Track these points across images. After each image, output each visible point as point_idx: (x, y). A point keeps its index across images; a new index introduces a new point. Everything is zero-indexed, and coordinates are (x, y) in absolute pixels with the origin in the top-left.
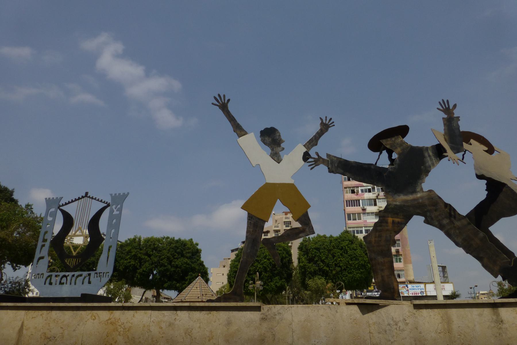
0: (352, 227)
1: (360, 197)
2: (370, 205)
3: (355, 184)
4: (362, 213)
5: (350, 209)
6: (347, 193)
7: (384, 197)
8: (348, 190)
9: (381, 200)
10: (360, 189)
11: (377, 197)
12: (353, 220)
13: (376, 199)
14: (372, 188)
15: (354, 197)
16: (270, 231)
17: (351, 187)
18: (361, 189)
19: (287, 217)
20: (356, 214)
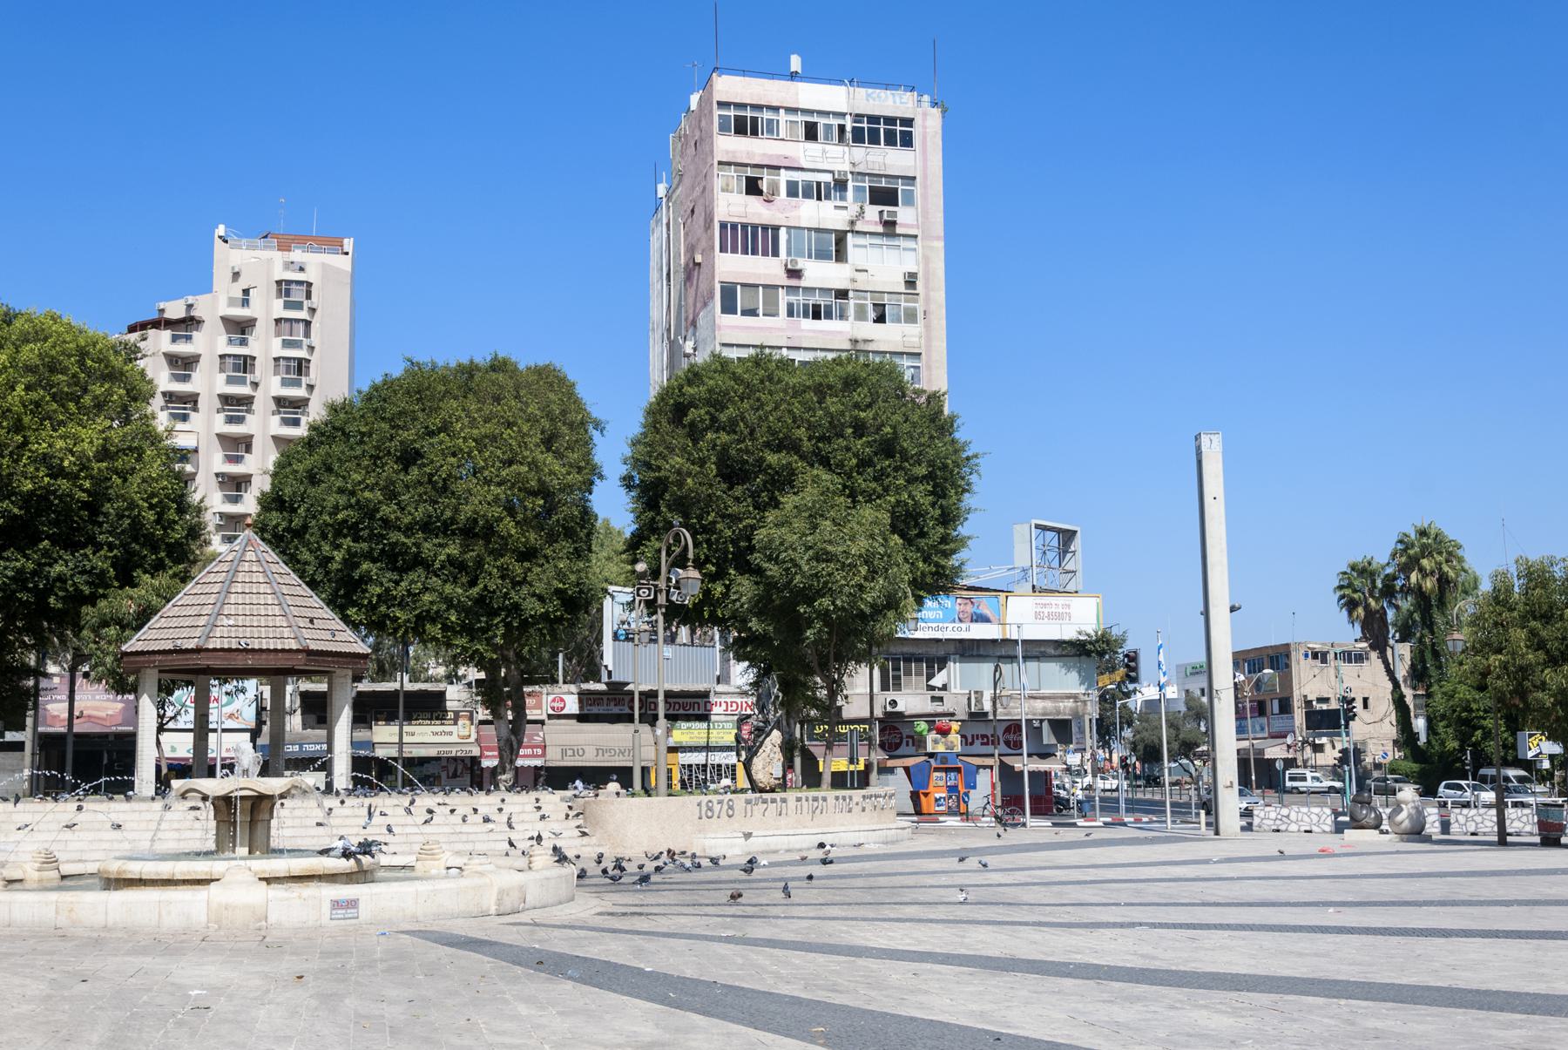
0: (738, 346)
1: (780, 216)
2: (822, 255)
3: (764, 154)
4: (783, 287)
5: (731, 266)
6: (725, 190)
7: (880, 229)
8: (733, 174)
9: (867, 240)
10: (784, 177)
11: (852, 223)
12: (742, 314)
13: (846, 232)
14: (835, 180)
15: (753, 210)
16: (204, 318)
17: (746, 165)
18: (788, 181)
19: (292, 263)
20: (761, 288)
